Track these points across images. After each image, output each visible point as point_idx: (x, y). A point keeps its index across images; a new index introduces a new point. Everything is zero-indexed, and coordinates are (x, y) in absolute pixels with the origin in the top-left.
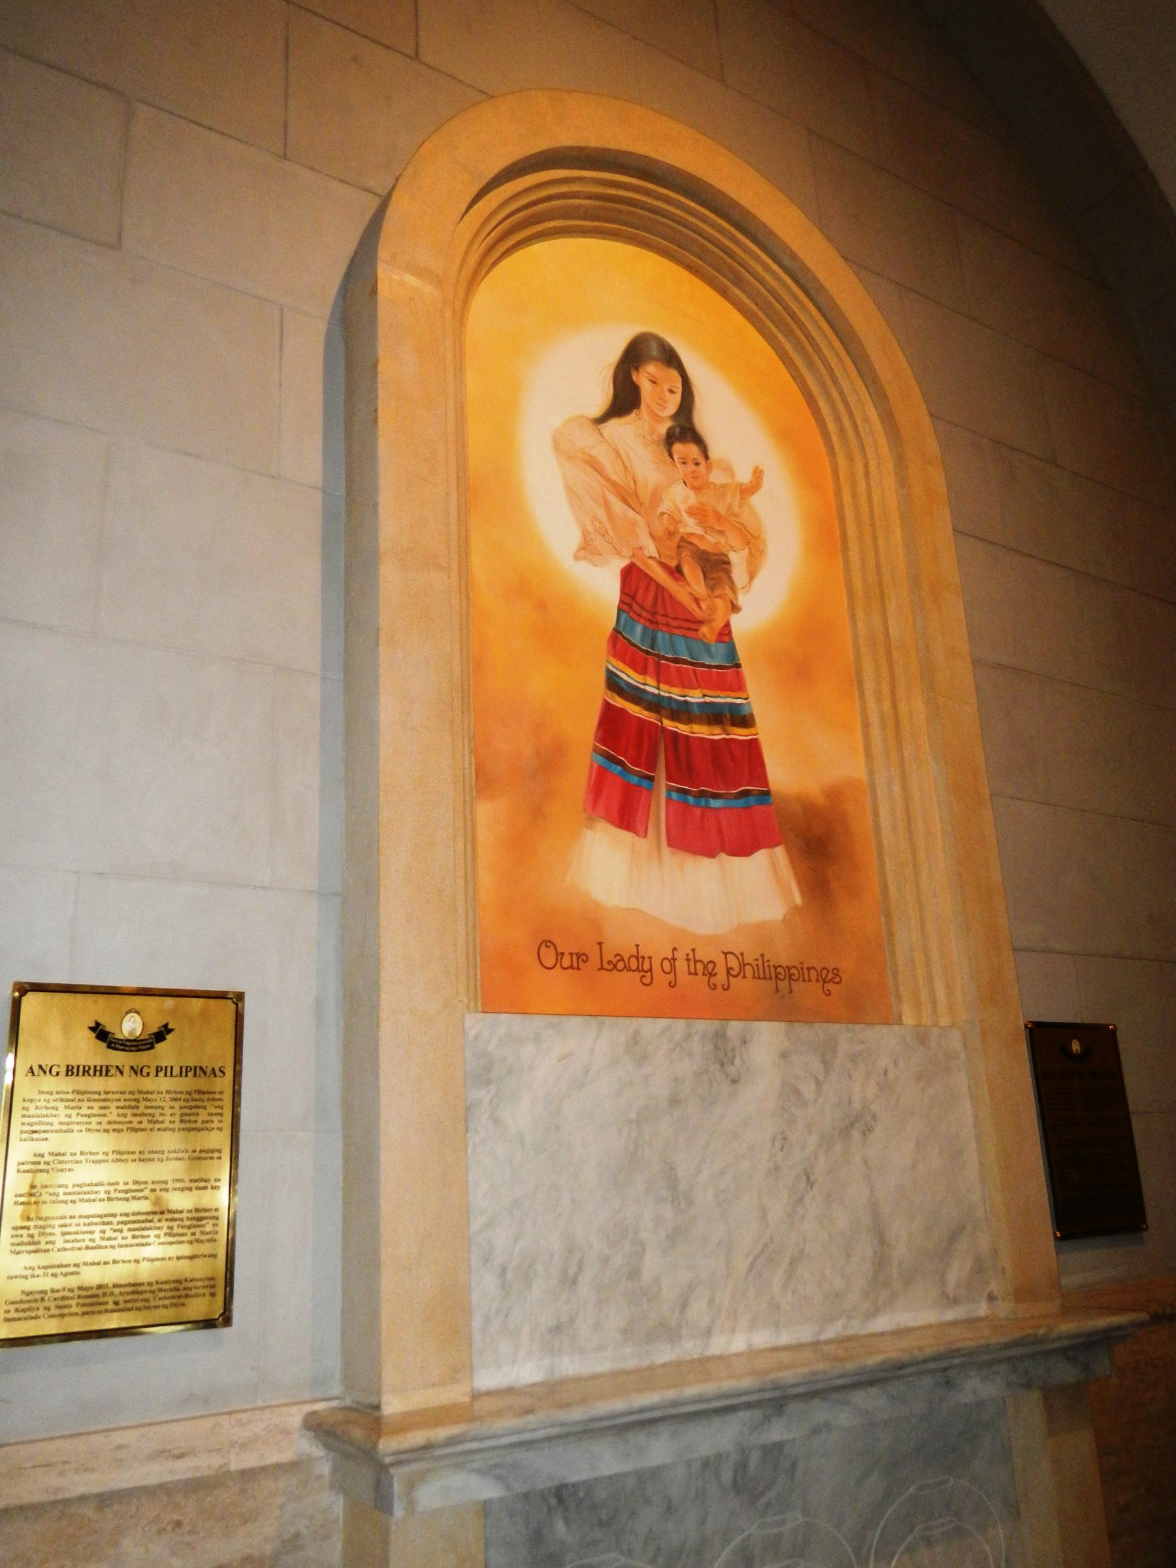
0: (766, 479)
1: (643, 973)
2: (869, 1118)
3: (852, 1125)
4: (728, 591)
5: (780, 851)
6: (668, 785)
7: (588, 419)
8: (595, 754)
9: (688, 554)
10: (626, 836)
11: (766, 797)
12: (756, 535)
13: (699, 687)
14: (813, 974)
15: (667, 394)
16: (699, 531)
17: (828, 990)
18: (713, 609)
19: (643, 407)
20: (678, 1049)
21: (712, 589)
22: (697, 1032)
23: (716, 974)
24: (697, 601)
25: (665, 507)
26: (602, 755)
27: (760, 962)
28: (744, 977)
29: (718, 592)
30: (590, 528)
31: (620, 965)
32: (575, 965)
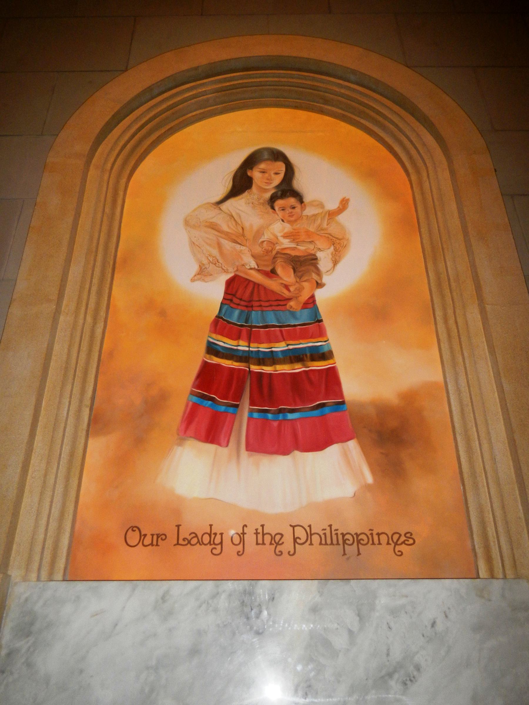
0: (351, 204)
1: (213, 546)
2: (411, 668)
3: (390, 675)
4: (314, 276)
5: (352, 445)
6: (250, 408)
7: (212, 204)
8: (191, 396)
9: (282, 261)
10: (211, 447)
11: (342, 406)
12: (340, 237)
13: (284, 340)
14: (384, 538)
15: (273, 176)
16: (293, 245)
17: (399, 551)
18: (300, 290)
19: (254, 188)
20: (204, 606)
21: (300, 278)
22: (224, 591)
23: (283, 543)
24: (287, 287)
25: (266, 236)
26: (196, 396)
27: (328, 532)
28: (311, 544)
29: (305, 278)
30: (205, 261)
31: (194, 541)
32: (155, 543)
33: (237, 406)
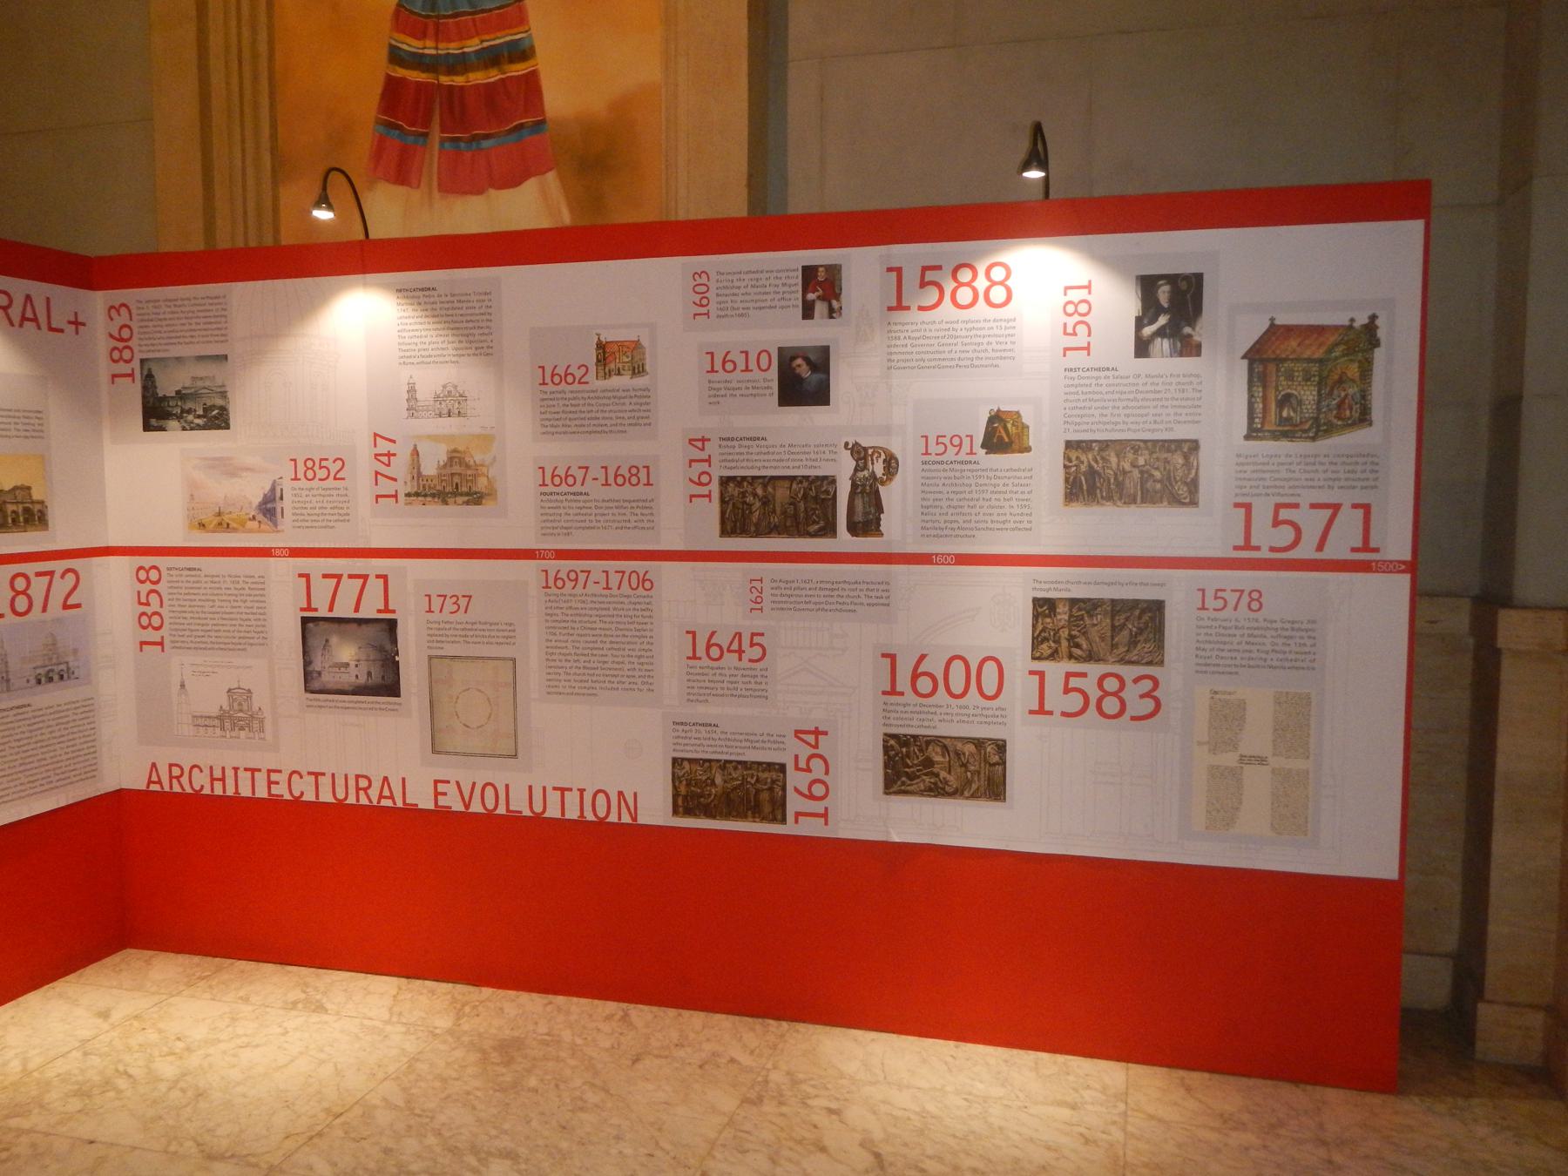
5: (551, 177)
10: (401, 190)
13: (478, 34)
33: (425, 135)
